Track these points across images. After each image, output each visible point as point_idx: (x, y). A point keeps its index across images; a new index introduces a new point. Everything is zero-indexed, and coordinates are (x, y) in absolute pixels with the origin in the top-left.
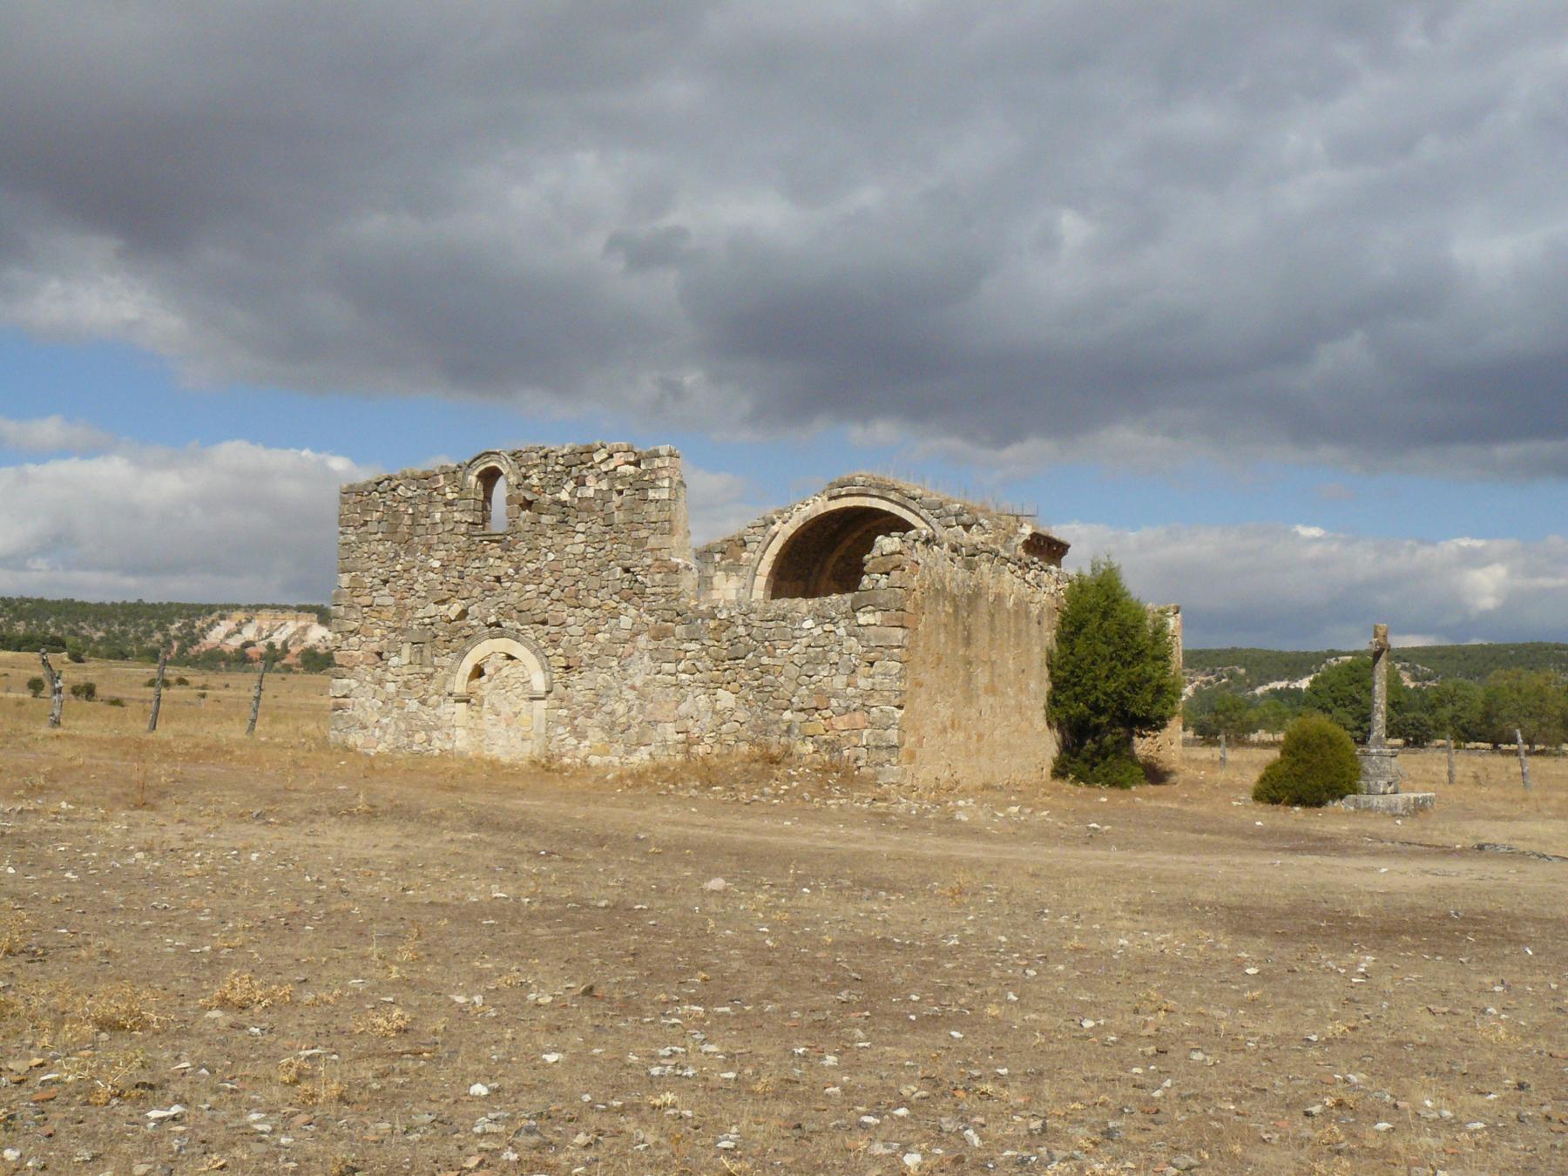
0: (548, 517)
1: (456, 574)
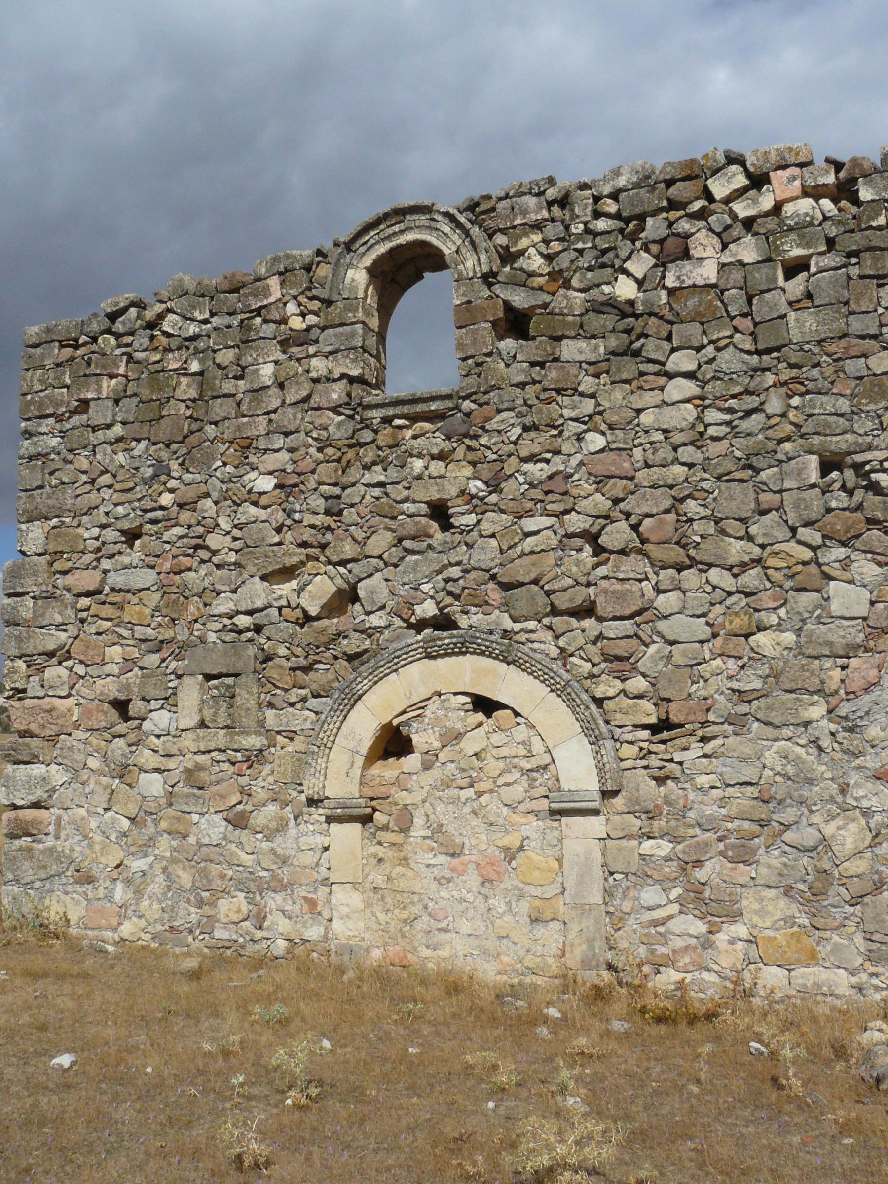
0: (582, 344)
1: (319, 503)
